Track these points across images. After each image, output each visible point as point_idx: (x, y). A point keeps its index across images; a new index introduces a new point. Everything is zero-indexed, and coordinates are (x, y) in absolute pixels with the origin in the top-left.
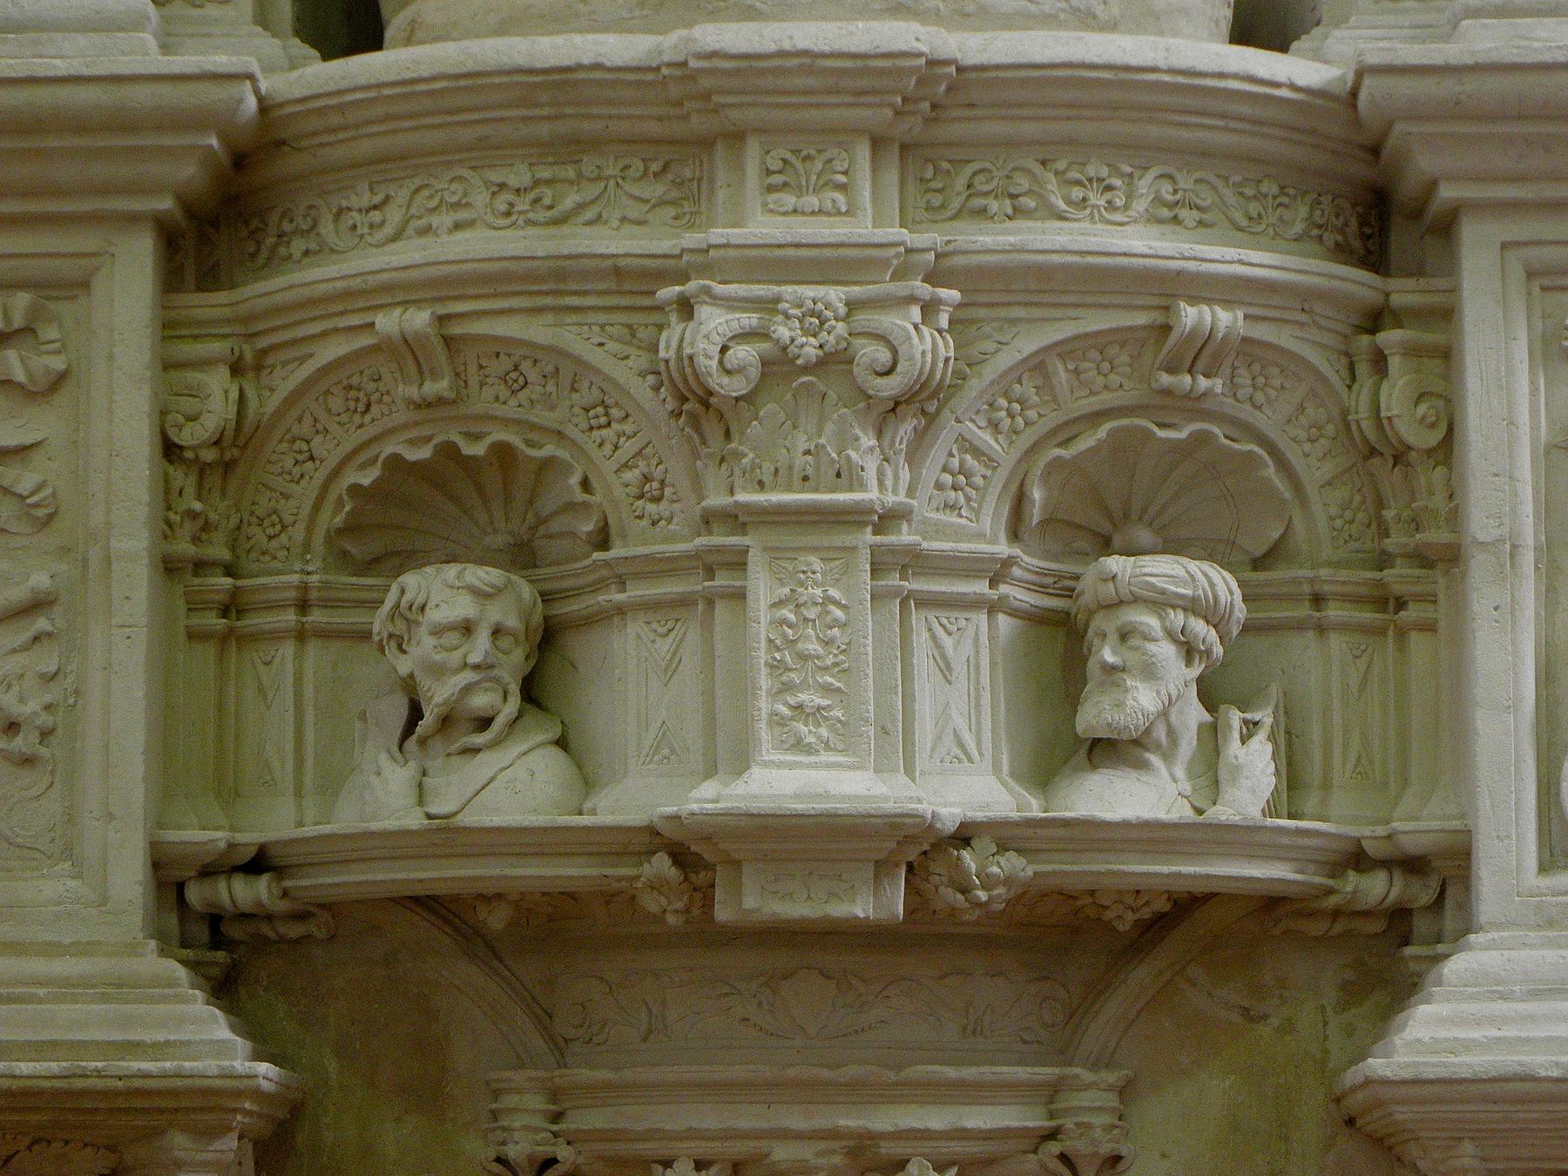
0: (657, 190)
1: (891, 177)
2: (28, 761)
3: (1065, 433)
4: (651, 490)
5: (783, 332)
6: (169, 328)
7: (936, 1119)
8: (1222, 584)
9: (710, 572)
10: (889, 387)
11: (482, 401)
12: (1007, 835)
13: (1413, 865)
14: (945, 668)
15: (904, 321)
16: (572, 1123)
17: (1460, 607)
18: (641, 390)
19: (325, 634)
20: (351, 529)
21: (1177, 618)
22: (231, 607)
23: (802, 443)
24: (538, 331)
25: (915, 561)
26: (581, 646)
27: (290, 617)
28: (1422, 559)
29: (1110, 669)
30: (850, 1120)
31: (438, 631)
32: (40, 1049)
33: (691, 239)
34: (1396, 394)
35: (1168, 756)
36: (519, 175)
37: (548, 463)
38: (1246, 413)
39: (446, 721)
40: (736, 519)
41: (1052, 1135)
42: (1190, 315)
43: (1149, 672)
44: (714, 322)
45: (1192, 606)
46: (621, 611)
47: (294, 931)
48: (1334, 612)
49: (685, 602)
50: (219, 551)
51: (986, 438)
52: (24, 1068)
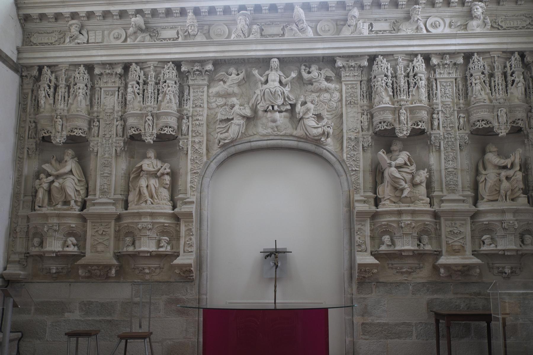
7: (153, 266)
8: (168, 239)
12: (155, 251)
15: (149, 225)
22: (119, 239)
24: (132, 225)
25: (151, 237)
42: (165, 224)
44: (140, 225)
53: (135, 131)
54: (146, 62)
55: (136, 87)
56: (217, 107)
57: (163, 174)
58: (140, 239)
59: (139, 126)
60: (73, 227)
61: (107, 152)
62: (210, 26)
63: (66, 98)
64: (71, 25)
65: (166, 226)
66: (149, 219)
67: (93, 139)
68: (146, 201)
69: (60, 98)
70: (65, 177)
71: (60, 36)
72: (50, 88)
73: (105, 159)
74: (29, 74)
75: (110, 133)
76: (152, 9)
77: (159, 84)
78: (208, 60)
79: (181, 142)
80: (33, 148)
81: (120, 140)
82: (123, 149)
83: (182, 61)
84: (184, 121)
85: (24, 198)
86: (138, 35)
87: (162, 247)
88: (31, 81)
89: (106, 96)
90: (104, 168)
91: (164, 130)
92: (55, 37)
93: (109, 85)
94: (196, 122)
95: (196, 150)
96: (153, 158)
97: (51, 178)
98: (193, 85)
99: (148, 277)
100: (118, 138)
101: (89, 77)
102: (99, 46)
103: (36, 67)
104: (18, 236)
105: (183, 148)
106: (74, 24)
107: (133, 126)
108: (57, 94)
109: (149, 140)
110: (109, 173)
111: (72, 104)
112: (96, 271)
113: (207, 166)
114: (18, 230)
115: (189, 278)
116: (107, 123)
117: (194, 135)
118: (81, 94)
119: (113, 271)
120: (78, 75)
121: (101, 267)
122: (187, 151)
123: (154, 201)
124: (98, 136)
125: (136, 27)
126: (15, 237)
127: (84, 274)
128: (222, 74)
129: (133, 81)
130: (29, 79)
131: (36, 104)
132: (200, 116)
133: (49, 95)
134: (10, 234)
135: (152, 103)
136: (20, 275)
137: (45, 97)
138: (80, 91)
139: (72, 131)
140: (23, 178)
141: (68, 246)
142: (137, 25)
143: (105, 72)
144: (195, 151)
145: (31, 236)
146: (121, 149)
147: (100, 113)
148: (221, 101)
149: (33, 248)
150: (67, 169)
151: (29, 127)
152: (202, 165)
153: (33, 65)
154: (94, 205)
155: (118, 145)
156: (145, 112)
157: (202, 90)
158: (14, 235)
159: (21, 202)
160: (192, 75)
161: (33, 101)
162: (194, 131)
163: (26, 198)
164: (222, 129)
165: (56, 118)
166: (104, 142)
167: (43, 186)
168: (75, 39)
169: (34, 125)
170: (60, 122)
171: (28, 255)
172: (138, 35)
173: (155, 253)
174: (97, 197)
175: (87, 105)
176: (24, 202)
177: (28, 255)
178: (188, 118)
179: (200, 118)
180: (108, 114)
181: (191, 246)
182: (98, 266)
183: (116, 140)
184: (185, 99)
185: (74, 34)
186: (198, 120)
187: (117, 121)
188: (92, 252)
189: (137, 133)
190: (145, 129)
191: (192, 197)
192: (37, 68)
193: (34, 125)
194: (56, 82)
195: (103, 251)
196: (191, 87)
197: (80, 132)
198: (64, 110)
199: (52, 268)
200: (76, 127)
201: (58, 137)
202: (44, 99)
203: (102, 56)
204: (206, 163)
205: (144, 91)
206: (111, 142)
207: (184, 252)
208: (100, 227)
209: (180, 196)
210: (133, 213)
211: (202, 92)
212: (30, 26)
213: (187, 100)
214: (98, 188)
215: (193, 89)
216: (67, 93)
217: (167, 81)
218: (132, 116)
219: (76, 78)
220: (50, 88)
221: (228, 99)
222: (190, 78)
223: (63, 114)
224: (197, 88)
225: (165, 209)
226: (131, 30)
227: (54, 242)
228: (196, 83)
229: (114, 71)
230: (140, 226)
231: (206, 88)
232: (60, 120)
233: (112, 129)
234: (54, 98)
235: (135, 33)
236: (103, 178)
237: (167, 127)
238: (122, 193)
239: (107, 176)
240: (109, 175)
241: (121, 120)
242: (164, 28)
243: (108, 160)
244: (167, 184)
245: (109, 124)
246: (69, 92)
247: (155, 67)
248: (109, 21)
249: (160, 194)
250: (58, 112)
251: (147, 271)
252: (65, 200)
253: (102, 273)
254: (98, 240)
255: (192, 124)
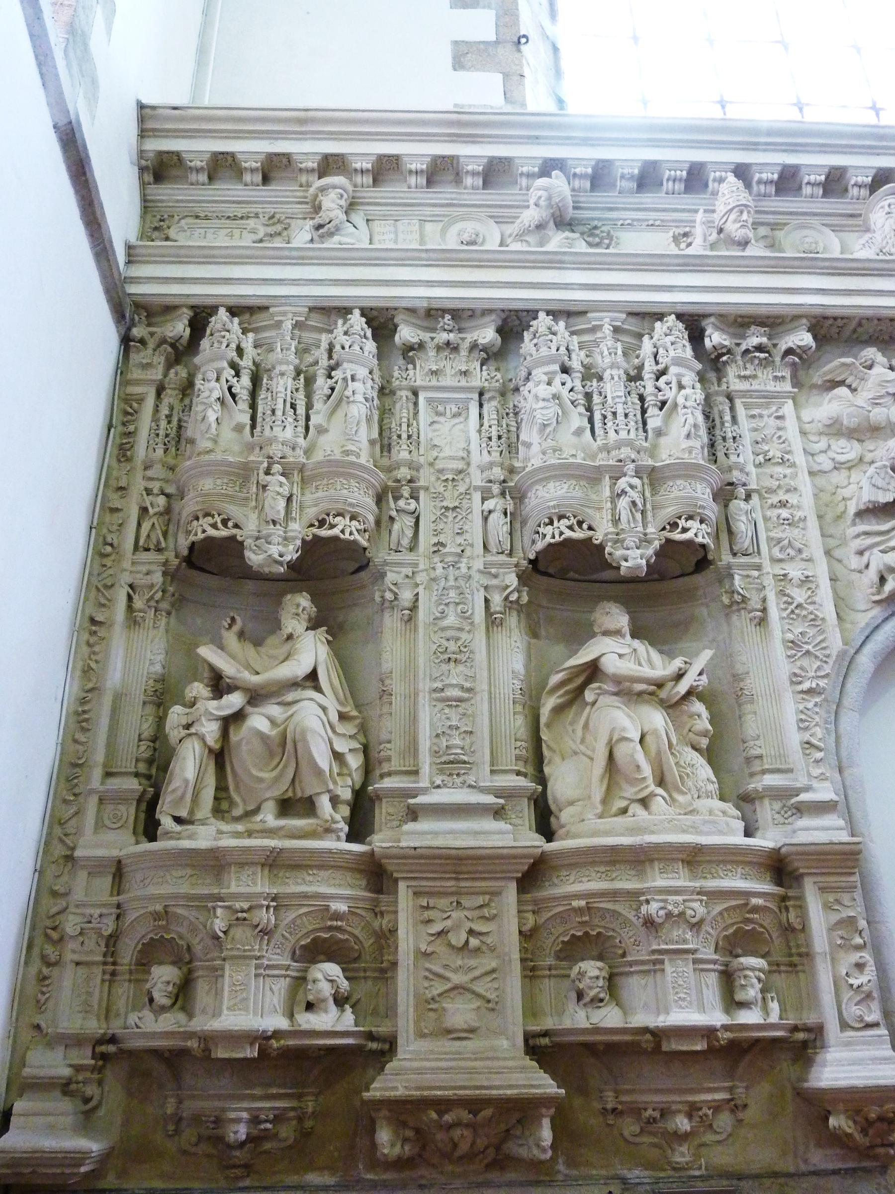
0: (633, 872)
1: (686, 870)
2: (493, 1010)
3: (726, 928)
4: (637, 943)
5: (670, 907)
6: (519, 902)
9: (654, 964)
10: (694, 920)
11: (596, 921)
12: (726, 1028)
13: (808, 1029)
14: (708, 986)
16: (624, 1098)
17: (813, 967)
18: (634, 919)
19: (555, 976)
20: (560, 950)
21: (757, 973)
23: (675, 933)
24: (610, 906)
26: (621, 981)
27: (548, 972)
28: (800, 955)
29: (742, 986)
30: (691, 1098)
31: (591, 978)
32: (510, 1087)
33: (646, 885)
34: (792, 915)
35: (756, 1005)
36: (602, 869)
37: (609, 937)
38: (761, 922)
39: (592, 1000)
40: (661, 952)
41: (732, 1100)
42: (755, 901)
43: (752, 986)
45: (760, 970)
46: (632, 973)
47: (550, 1050)
48: (782, 968)
49: (648, 971)
50: (529, 956)
51: (711, 931)
52: (509, 1092)
53: (570, 528)
54: (585, 313)
55: (563, 384)
56: (835, 468)
57: (689, 693)
58: (655, 966)
59: (589, 511)
60: (337, 916)
61: (452, 606)
62: (774, 227)
63: (301, 410)
64: (323, 190)
65: (756, 909)
66: (680, 879)
67: (394, 557)
68: (644, 802)
69: (280, 406)
70: (290, 697)
71: (270, 230)
72: (237, 375)
73: (449, 633)
74: (152, 334)
75: (459, 540)
76: (599, 161)
77: (642, 379)
78: (796, 317)
79: (737, 577)
80: (152, 586)
81: (502, 565)
82: (514, 597)
83: (710, 315)
84: (738, 505)
85: (102, 783)
86: (550, 233)
87: (743, 1005)
88: (159, 360)
89: (436, 419)
90: (445, 667)
91: (685, 530)
92: (253, 231)
93: (448, 381)
94: (780, 511)
95: (799, 606)
96: (628, 637)
97: (234, 701)
98: (745, 394)
99: (682, 1155)
100: (490, 558)
101: (375, 350)
102: (424, 255)
103: (185, 310)
104: (69, 956)
105: (744, 599)
106: (335, 187)
107: (563, 510)
108: (262, 394)
109: (639, 561)
110: (467, 685)
111: (321, 431)
112: (457, 1133)
113: (847, 663)
114: (71, 925)
115: (881, 1151)
116: (445, 504)
117: (781, 556)
118: (359, 397)
119: (546, 1134)
120: (343, 339)
121: (487, 1112)
122: (764, 610)
123: (673, 800)
124: (412, 549)
125: (550, 206)
126: (53, 958)
127: (397, 1150)
128: (844, 364)
129: (550, 360)
130: (150, 351)
131: (173, 433)
132: (788, 491)
133: (233, 396)
134: (30, 947)
135: (632, 435)
136: (76, 1158)
137: (221, 401)
138: (357, 386)
139: (322, 523)
140: (107, 701)
141: (310, 1007)
142: (556, 200)
143: (432, 339)
144: (794, 611)
145: (127, 953)
146: (506, 598)
147: (418, 470)
148: (848, 450)
149: (147, 1014)
150: (299, 667)
151: (144, 510)
152: (831, 661)
153: (177, 301)
154: (413, 814)
155: (495, 582)
156: (611, 462)
157: (777, 411)
158: (49, 950)
159: (93, 801)
160: (740, 363)
161: (163, 423)
162: (779, 541)
163: (115, 783)
164: (878, 539)
165: (267, 473)
166: (439, 571)
167: (203, 730)
168: (331, 234)
169: (161, 501)
170: (281, 485)
171: (112, 1048)
172: (550, 233)
173: (728, 1035)
174: (424, 783)
175: (372, 442)
176: (101, 800)
177: (112, 1048)
178: (748, 497)
179: (793, 499)
180: (450, 477)
181: (869, 996)
182: (474, 1105)
183: (486, 565)
184: (729, 435)
185: (332, 215)
186: (783, 504)
187: (484, 500)
188: (421, 1035)
189: (578, 535)
190: (616, 521)
191: (815, 784)
192: (187, 314)
193: (161, 501)
194: (258, 359)
195: (472, 1030)
196: (738, 403)
197: (354, 529)
198: (294, 449)
199: (232, 1115)
200: (340, 506)
201: (275, 539)
202: (217, 407)
203: (430, 284)
204: (842, 654)
205: (588, 396)
206: (464, 570)
207: (844, 1025)
208: (454, 914)
209: (770, 780)
210: (614, 849)
211: (778, 418)
212: (166, 193)
213: (734, 438)
214: (425, 744)
215: (747, 406)
216: (302, 390)
217: (673, 370)
218: (556, 477)
219: (338, 348)
220: (237, 375)
221: (870, 445)
222: (732, 372)
223: (291, 459)
224: (759, 406)
225: (731, 832)
226: (530, 216)
227: (257, 988)
228: (757, 387)
229: (463, 339)
230: (653, 908)
231: (788, 408)
232: (283, 479)
233: (466, 527)
234: (253, 406)
235: (540, 227)
236: (440, 705)
237: (690, 518)
238: (523, 770)
239: (460, 700)
240: (466, 695)
241: (503, 494)
242: (630, 226)
243: (458, 639)
244: (705, 734)
245: (456, 507)
246: (309, 396)
247: (616, 330)
248: (445, 193)
249: (688, 770)
250: (276, 450)
251: (683, 1124)
252: (290, 794)
253: (481, 1143)
254: (448, 974)
255: (766, 519)
